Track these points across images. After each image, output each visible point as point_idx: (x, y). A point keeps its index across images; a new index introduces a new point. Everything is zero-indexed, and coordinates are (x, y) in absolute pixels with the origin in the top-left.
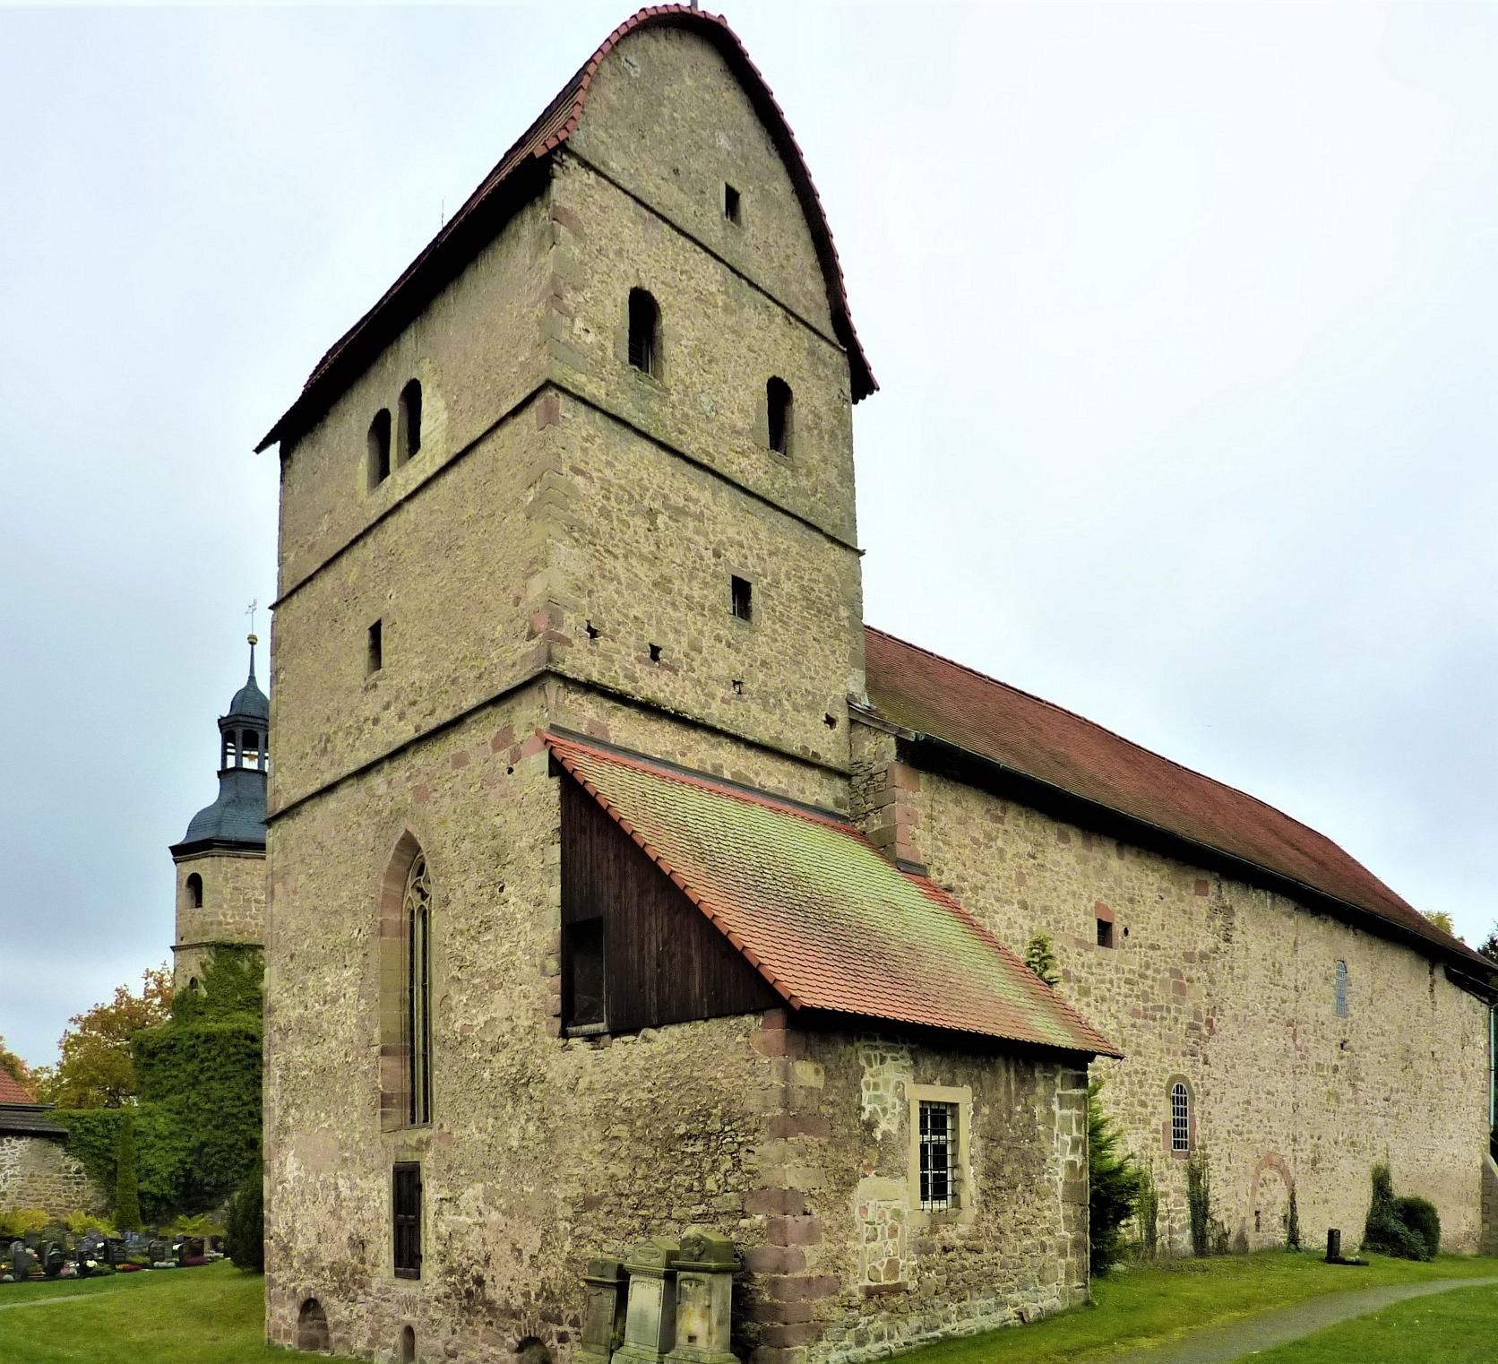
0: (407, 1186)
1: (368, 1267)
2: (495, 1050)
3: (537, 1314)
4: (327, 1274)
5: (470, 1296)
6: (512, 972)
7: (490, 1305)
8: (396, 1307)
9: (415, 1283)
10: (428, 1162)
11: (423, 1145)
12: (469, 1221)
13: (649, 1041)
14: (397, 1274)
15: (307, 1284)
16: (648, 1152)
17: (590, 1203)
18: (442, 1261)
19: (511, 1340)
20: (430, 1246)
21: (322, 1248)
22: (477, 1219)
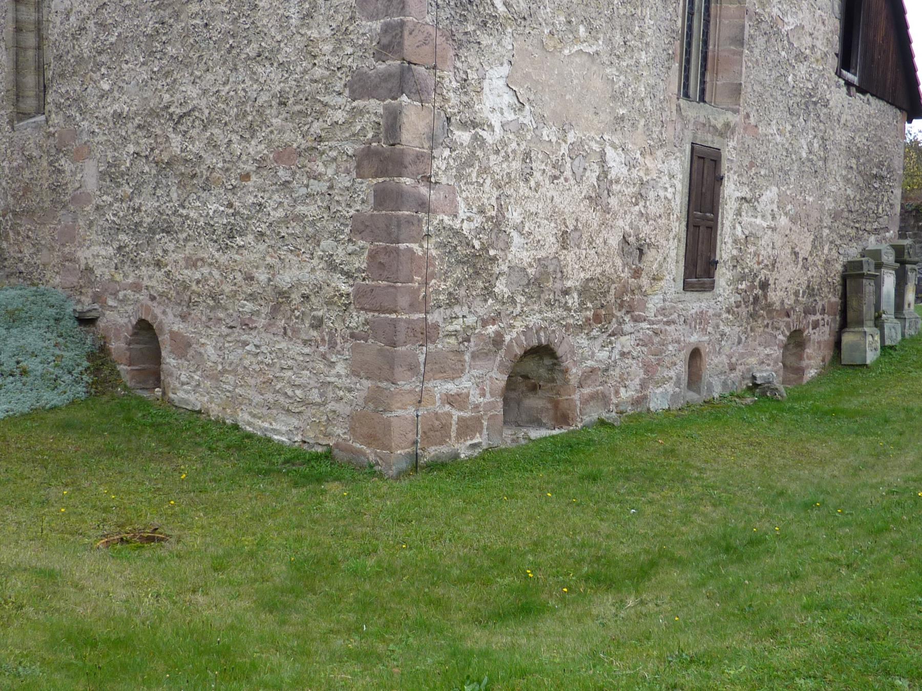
2: (801, 57)
4: (573, 300)
9: (708, 295)
10: (730, 151)
11: (727, 130)
13: (869, 104)
14: (687, 287)
15: (524, 325)
17: (836, 216)
20: (725, 251)
21: (569, 257)
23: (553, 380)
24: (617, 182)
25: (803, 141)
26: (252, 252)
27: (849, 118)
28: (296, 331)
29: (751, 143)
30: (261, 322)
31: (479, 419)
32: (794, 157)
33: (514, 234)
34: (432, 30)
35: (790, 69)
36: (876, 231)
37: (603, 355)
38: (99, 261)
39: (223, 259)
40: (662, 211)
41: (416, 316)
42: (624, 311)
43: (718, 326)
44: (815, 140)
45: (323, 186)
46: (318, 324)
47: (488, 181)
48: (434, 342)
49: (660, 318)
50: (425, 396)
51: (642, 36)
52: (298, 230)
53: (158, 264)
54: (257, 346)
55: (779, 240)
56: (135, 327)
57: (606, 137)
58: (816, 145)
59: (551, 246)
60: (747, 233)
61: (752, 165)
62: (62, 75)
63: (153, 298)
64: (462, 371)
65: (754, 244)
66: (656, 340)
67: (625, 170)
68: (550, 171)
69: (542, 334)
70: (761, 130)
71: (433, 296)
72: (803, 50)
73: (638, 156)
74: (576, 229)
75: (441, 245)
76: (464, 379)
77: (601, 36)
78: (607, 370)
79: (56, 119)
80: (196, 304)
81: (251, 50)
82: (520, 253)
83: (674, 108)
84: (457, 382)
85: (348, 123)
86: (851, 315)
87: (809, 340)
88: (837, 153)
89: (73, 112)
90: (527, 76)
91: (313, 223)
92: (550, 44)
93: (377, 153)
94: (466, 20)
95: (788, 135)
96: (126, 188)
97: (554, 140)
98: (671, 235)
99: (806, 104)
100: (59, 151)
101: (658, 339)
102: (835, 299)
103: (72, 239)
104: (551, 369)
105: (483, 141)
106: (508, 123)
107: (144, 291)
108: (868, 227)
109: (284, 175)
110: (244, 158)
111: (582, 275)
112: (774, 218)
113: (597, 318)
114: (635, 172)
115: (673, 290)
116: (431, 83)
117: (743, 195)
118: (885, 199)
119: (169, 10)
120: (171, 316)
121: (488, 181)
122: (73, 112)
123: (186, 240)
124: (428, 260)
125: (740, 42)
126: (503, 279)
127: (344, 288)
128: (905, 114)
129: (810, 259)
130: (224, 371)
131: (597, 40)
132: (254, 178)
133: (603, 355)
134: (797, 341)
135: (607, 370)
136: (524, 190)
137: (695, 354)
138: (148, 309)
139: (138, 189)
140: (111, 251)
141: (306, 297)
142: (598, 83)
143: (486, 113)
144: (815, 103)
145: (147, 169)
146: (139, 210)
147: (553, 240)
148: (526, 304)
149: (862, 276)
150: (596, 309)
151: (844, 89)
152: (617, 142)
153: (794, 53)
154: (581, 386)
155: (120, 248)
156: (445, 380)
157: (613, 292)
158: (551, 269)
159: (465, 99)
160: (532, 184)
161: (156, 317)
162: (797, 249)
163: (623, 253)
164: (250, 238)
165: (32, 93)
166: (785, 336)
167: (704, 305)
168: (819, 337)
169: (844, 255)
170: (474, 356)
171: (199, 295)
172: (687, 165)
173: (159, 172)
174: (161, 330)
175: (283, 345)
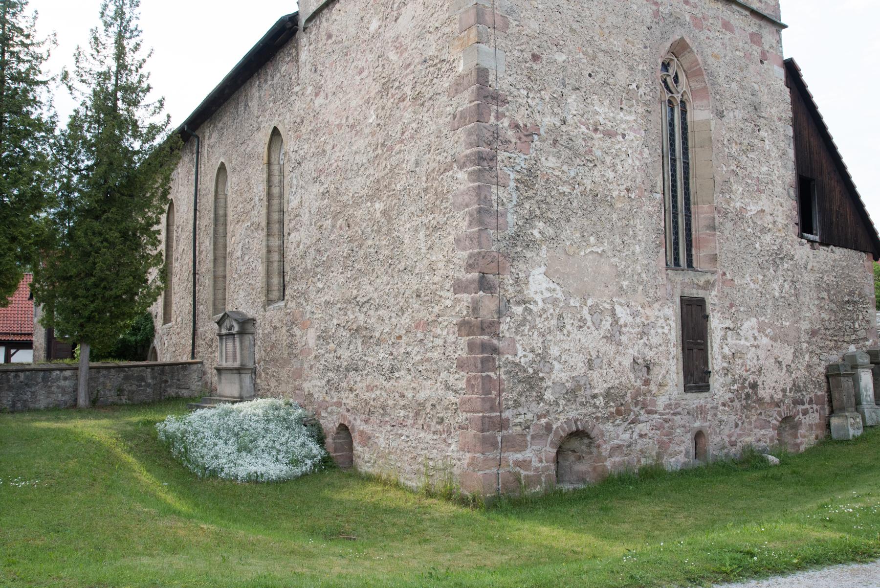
0: (694, 318)
1: (653, 388)
2: (764, 230)
3: (791, 402)
5: (748, 394)
6: (770, 186)
7: (760, 401)
8: (687, 418)
9: (705, 394)
10: (712, 298)
11: (708, 286)
12: (748, 344)
13: (833, 252)
14: (687, 389)
15: (564, 418)
16: (833, 306)
17: (814, 333)
18: (726, 374)
19: (774, 422)
20: (716, 363)
21: (595, 375)
22: (752, 342)
23: (591, 453)
24: (626, 326)
25: (774, 285)
26: (404, 380)
27: (815, 264)
28: (429, 426)
29: (729, 291)
30: (410, 422)
31: (539, 476)
32: (767, 296)
33: (555, 363)
34: (495, 254)
35: (757, 239)
36: (855, 341)
37: (627, 436)
38: (317, 389)
39: (388, 385)
40: (661, 342)
41: (494, 414)
42: (639, 407)
43: (715, 415)
44: (786, 283)
45: (440, 342)
46: (441, 421)
47: (536, 333)
48: (506, 429)
49: (668, 411)
50: (503, 463)
51: (635, 236)
52: (428, 367)
53: (351, 390)
54: (408, 437)
55: (762, 354)
56: (337, 429)
57: (614, 300)
58: (786, 286)
59: (581, 368)
60: (733, 351)
61: (732, 306)
62: (295, 279)
63: (348, 411)
64: (526, 446)
65: (741, 358)
66: (667, 425)
67: (630, 319)
68: (577, 323)
69: (579, 423)
70: (737, 281)
71: (504, 402)
72: (766, 225)
73: (639, 308)
74: (598, 357)
75: (507, 372)
76: (528, 451)
77: (606, 241)
78: (629, 446)
79: (292, 305)
80: (373, 413)
81: (401, 267)
82: (559, 374)
83: (664, 276)
84: (523, 453)
85: (453, 307)
86: (835, 403)
87: (801, 423)
88: (808, 290)
89: (302, 300)
90: (557, 271)
91: (436, 363)
92: (571, 251)
93: (468, 323)
94: (516, 245)
95: (760, 282)
96: (332, 345)
97: (578, 305)
98: (671, 357)
99: (774, 260)
100: (293, 323)
101: (668, 425)
102: (822, 393)
103: (300, 376)
104: (589, 446)
105: (531, 310)
106: (546, 299)
107: (343, 406)
108: (847, 339)
109: (420, 336)
110: (398, 326)
111: (605, 385)
112: (755, 338)
113: (619, 413)
114: (638, 320)
115: (676, 392)
116: (496, 282)
117: (727, 325)
118: (861, 317)
119: (356, 244)
120: (359, 421)
121: (536, 333)
122: (302, 300)
123: (367, 375)
124: (500, 381)
125: (714, 228)
126: (549, 391)
127: (454, 400)
128: (871, 255)
129: (793, 365)
130: (390, 453)
131: (603, 243)
132: (404, 338)
133: (627, 436)
134: (788, 422)
135: (629, 446)
136: (559, 336)
137: (699, 435)
138: (345, 417)
139: (339, 345)
140: (324, 382)
141: (433, 406)
142: (607, 268)
143: (532, 295)
144: (782, 259)
145: (344, 334)
146: (339, 358)
147: (582, 365)
148: (566, 405)
149: (839, 375)
150: (617, 406)
151: (808, 245)
152: (623, 302)
153: (758, 228)
154: (610, 456)
155: (329, 381)
156: (515, 451)
157: (629, 395)
158: (582, 383)
159: (518, 289)
160: (565, 332)
161: (350, 422)
162: (780, 359)
163: (634, 370)
164: (403, 373)
165: (276, 288)
166: (778, 421)
167: (702, 402)
168: (810, 420)
169: (826, 361)
170: (533, 437)
171: (375, 408)
172: (679, 311)
173: (351, 335)
174: (353, 429)
175: (422, 435)
